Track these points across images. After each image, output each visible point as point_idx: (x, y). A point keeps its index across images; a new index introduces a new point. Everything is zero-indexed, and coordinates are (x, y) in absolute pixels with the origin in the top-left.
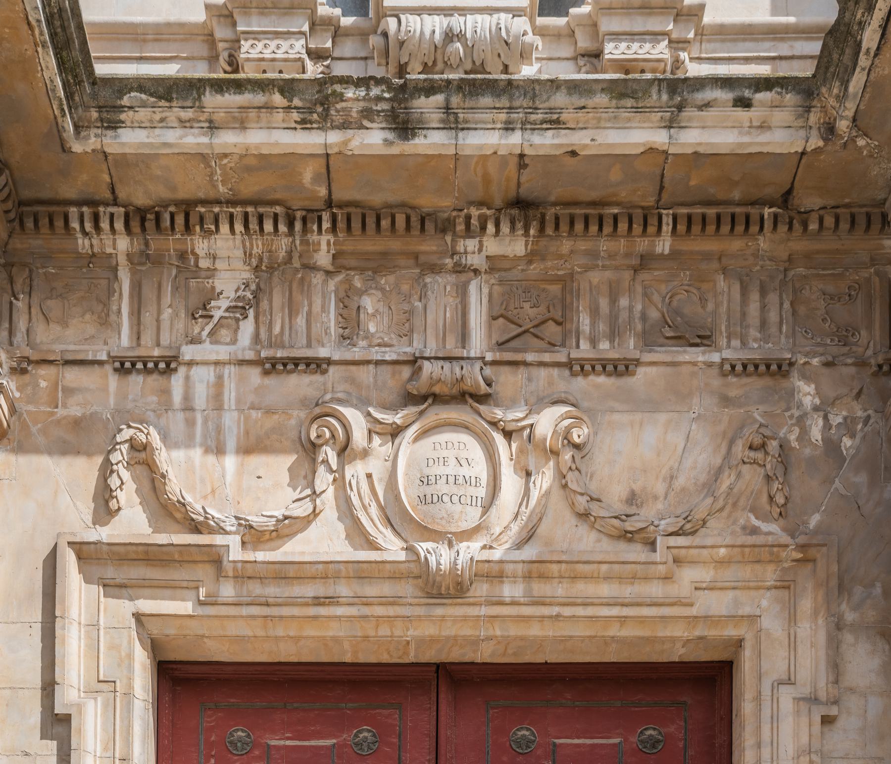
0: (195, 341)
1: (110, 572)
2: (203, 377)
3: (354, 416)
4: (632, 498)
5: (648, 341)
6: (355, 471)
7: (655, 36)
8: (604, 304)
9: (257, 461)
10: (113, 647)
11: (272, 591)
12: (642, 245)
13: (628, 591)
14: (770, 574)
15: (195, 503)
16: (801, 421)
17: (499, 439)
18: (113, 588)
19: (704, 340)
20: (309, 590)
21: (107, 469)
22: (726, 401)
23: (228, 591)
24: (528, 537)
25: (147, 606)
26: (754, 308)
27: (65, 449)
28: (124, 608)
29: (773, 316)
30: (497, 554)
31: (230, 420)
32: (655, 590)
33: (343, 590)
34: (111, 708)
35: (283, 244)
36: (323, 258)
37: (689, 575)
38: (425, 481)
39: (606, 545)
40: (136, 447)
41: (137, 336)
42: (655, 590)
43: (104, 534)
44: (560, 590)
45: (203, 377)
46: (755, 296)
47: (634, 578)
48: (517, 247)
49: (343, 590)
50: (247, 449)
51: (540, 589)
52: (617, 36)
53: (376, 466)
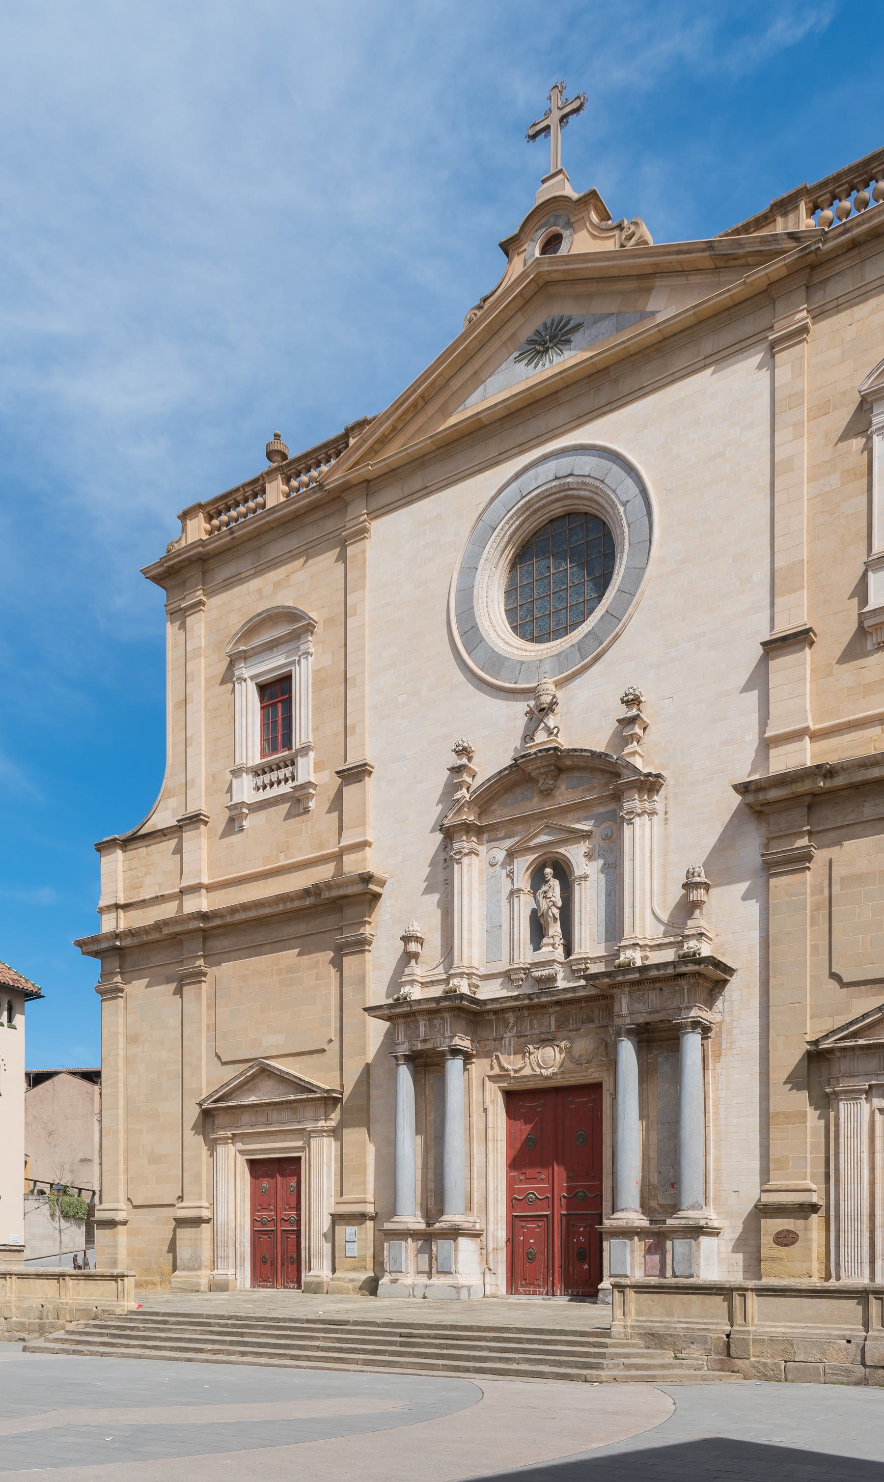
0: (506, 1033)
1: (494, 1079)
2: (508, 1039)
3: (531, 1047)
4: (580, 1056)
5: (583, 1023)
6: (532, 1057)
7: (581, 964)
8: (574, 1017)
9: (516, 1056)
10: (495, 1093)
11: (520, 1080)
12: (580, 1005)
13: (580, 1074)
14: (605, 1068)
15: (506, 1065)
16: (610, 1037)
17: (555, 1047)
18: (494, 1082)
19: (593, 1022)
20: (525, 1080)
21: (492, 1061)
22: (597, 1034)
23: (512, 1081)
24: (561, 1066)
25: (500, 1085)
26: (601, 1014)
27: (486, 1057)
28: (497, 1085)
29: (604, 1016)
30: (556, 1070)
31: (512, 1048)
32: (585, 1074)
33: (531, 1079)
34: (494, 1105)
35: (519, 1013)
36: (526, 1015)
37: (591, 1070)
38: (543, 1057)
39: (575, 1066)
40: (496, 1056)
41: (496, 1033)
42: (585, 1074)
43: (491, 1073)
44: (568, 1075)
45: (508, 1039)
46: (601, 1012)
47: (579, 1072)
48: (558, 1009)
49: (531, 1079)
50: (515, 1054)
51: (565, 1076)
52: (574, 965)
53: (535, 1055)
